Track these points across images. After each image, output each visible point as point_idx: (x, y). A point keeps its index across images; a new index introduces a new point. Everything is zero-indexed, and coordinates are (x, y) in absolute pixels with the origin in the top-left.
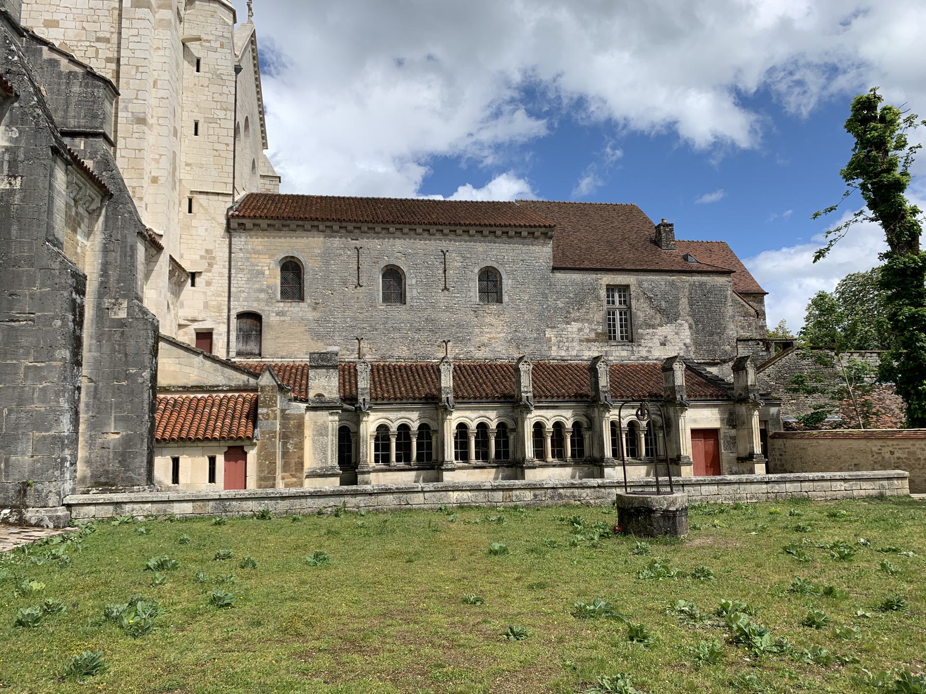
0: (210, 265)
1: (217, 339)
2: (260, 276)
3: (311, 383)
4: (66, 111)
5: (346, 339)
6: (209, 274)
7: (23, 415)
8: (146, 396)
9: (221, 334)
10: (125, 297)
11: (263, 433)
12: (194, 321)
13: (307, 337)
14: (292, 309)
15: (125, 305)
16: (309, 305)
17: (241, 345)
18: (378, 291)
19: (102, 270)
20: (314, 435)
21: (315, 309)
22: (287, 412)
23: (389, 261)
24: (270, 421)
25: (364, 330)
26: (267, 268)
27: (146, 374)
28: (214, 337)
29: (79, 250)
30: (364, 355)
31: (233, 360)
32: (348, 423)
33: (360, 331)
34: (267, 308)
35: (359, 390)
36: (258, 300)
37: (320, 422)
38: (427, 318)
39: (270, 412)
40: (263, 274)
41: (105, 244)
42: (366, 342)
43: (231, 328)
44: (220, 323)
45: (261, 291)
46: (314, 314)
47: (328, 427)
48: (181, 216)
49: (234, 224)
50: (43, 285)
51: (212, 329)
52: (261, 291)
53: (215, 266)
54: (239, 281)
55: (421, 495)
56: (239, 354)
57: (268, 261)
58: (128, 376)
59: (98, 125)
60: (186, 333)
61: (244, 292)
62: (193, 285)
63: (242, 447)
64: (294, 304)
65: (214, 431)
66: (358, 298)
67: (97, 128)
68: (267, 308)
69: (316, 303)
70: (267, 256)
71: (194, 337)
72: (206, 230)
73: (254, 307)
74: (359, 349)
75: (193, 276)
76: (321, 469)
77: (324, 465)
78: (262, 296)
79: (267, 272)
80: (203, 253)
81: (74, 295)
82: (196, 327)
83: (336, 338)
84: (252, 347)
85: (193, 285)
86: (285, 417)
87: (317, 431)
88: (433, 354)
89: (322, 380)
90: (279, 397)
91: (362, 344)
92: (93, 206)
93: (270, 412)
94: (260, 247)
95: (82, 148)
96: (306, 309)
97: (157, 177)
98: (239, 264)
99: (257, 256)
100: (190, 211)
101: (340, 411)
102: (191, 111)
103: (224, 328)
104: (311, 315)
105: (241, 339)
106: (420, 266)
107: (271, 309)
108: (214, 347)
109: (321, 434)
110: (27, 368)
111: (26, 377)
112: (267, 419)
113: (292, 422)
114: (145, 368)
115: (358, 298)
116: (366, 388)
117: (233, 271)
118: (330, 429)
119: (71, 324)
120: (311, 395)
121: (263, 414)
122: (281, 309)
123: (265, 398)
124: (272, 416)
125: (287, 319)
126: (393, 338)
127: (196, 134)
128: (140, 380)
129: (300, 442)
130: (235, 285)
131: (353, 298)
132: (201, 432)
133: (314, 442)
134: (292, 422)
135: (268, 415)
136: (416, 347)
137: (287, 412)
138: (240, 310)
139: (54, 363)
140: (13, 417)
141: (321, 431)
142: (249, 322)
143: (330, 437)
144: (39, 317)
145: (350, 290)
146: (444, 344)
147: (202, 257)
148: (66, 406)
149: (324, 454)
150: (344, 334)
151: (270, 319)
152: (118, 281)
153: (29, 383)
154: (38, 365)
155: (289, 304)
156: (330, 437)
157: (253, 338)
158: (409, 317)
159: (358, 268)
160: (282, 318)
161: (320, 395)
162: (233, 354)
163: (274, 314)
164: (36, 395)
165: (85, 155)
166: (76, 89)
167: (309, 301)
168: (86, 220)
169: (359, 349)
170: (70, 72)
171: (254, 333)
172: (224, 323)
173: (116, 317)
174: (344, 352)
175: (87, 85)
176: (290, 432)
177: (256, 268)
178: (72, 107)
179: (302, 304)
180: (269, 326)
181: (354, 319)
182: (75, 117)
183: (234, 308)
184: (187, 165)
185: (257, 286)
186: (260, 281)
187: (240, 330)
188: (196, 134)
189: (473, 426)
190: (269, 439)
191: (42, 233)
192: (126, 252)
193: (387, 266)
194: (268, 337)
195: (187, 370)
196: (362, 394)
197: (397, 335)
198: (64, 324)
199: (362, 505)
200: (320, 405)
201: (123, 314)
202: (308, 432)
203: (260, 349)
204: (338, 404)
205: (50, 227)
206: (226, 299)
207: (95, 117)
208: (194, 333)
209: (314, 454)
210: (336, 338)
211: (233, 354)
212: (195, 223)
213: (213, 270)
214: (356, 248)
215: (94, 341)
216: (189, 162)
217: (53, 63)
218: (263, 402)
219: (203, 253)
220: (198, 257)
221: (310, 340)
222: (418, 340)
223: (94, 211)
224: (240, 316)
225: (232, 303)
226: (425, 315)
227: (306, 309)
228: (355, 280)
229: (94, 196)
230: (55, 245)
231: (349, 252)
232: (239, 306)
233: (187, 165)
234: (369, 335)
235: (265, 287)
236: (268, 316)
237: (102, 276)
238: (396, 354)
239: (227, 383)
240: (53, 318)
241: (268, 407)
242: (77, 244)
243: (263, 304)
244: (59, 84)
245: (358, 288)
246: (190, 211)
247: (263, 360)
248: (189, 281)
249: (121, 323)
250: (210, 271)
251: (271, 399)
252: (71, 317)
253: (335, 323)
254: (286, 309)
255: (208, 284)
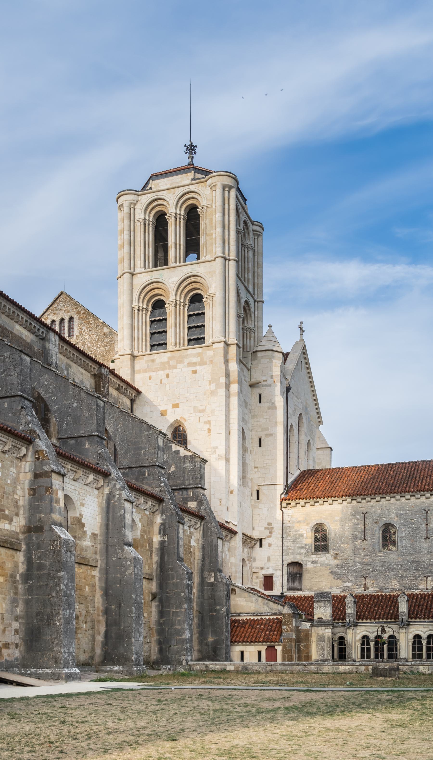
0: (271, 533)
1: (276, 580)
2: (301, 538)
3: (315, 610)
4: (184, 477)
5: (356, 577)
6: (270, 539)
7: (173, 630)
8: (224, 620)
9: (278, 577)
10: (213, 571)
11: (284, 639)
12: (262, 569)
13: (331, 577)
14: (320, 559)
15: (213, 575)
16: (332, 556)
17: (290, 584)
18: (379, 542)
19: (202, 558)
20: (317, 641)
21: (335, 558)
22: (300, 628)
23: (386, 521)
24: (288, 633)
25: (368, 571)
26: (305, 532)
27: (224, 609)
28: (274, 579)
29: (192, 550)
30: (368, 588)
31: (285, 594)
32: (344, 634)
33: (365, 571)
34: (305, 559)
35: (347, 614)
36: (300, 554)
37: (321, 633)
38: (413, 561)
39: (288, 628)
40: (302, 535)
41: (203, 545)
42: (370, 579)
43: (284, 573)
44: (277, 570)
45: (301, 548)
46: (335, 561)
47: (325, 636)
48: (253, 502)
49: (284, 504)
50: (177, 579)
51: (273, 574)
52: (301, 548)
53: (273, 533)
54: (288, 542)
55: (327, 667)
56: (289, 589)
57: (306, 527)
58: (216, 611)
59: (198, 482)
60: (257, 578)
61: (291, 549)
62: (261, 546)
63: (274, 646)
64: (322, 555)
65: (260, 638)
66: (364, 549)
67: (197, 484)
68: (305, 559)
69: (337, 554)
70: (305, 524)
71: (263, 579)
72: (268, 510)
73: (298, 559)
74: (365, 584)
75: (261, 540)
76: (321, 660)
77: (323, 658)
78: (303, 551)
79: (305, 535)
80: (266, 525)
81: (188, 582)
82: (263, 573)
83: (349, 577)
84: (297, 585)
85: (261, 546)
86: (298, 630)
87: (319, 638)
88: (417, 586)
89: (322, 609)
90: (294, 620)
91: (367, 581)
92: (197, 526)
93: (288, 628)
94: (300, 519)
95: (191, 495)
96: (330, 559)
97: (233, 490)
98: (288, 530)
99: (298, 524)
100: (258, 498)
101: (332, 627)
102: (257, 431)
103: (279, 573)
104: (334, 562)
105: (290, 579)
106: (409, 523)
107: (308, 559)
108: (274, 585)
109: (321, 641)
110: (173, 612)
111: (173, 615)
112: (287, 632)
113: (302, 633)
114: (223, 606)
115: (364, 549)
116: (351, 613)
117: (284, 536)
118: (326, 638)
119: (187, 594)
120: (315, 618)
121: (284, 629)
122: (314, 559)
123: (285, 620)
124: (289, 630)
125: (318, 565)
126: (388, 575)
127: (260, 446)
128: (221, 612)
129: (307, 645)
130: (286, 545)
131: (360, 549)
132: (254, 638)
133: (317, 644)
134: (302, 633)
135: (287, 629)
136: (404, 581)
137: (300, 628)
138: (290, 561)
139: (182, 610)
140: (170, 631)
141: (321, 639)
142: (294, 570)
143: (326, 642)
144: (176, 592)
145: (358, 543)
146: (425, 578)
147: (266, 528)
148: (187, 627)
149: (323, 652)
150: (355, 574)
151: (308, 566)
152: (210, 563)
153: (174, 618)
154: (177, 611)
155: (319, 556)
156: (326, 642)
157: (297, 578)
158: (400, 560)
159: (365, 527)
160: (315, 565)
161: (320, 619)
162: (285, 590)
163: (310, 563)
164: (177, 622)
165: (193, 499)
166: (188, 465)
167: (332, 553)
168: (194, 534)
169: (365, 584)
170: (185, 456)
171: (298, 575)
172: (279, 570)
173: (210, 581)
174: (355, 587)
175: (192, 463)
176: (301, 639)
177: (299, 533)
178: (186, 474)
179: (327, 555)
180: (307, 571)
181: (362, 563)
182: (187, 480)
183: (285, 560)
184: (255, 468)
185: (299, 545)
186: (301, 541)
187: (289, 574)
188: (260, 446)
189: (424, 636)
190: (288, 642)
191: (175, 557)
192: (213, 549)
193: (385, 524)
194: (306, 577)
195: (250, 604)
196: (349, 617)
197: (391, 573)
198: (185, 594)
199: (301, 670)
200: (321, 622)
201: (212, 580)
202: (314, 639)
203: (301, 586)
204: (330, 623)
205: (178, 554)
206: (281, 554)
207: (196, 478)
208: (262, 576)
209: (317, 652)
210: (349, 577)
211: (285, 590)
212: (261, 506)
213: (272, 536)
214: (363, 513)
215: (200, 594)
216: (256, 466)
217: (178, 452)
218: (284, 623)
219: (266, 525)
220: (263, 529)
221: (333, 579)
222: (406, 577)
223: (198, 528)
224: (289, 565)
225: (284, 557)
226: (412, 558)
227: (330, 559)
228: (362, 536)
229: (197, 522)
230: (180, 561)
231: (358, 517)
232: (289, 559)
233: (255, 468)
234: (371, 574)
235: (304, 545)
236: (306, 564)
237: (202, 561)
238: (390, 587)
239: (270, 611)
240: (181, 592)
241: (287, 625)
242: (191, 547)
243: (303, 556)
244: (180, 463)
245: (365, 541)
246: (258, 498)
247: (303, 593)
248: (258, 544)
249: (212, 584)
250: (270, 537)
251: (288, 621)
252: (187, 591)
253: (349, 566)
254: (317, 559)
255: (270, 545)
